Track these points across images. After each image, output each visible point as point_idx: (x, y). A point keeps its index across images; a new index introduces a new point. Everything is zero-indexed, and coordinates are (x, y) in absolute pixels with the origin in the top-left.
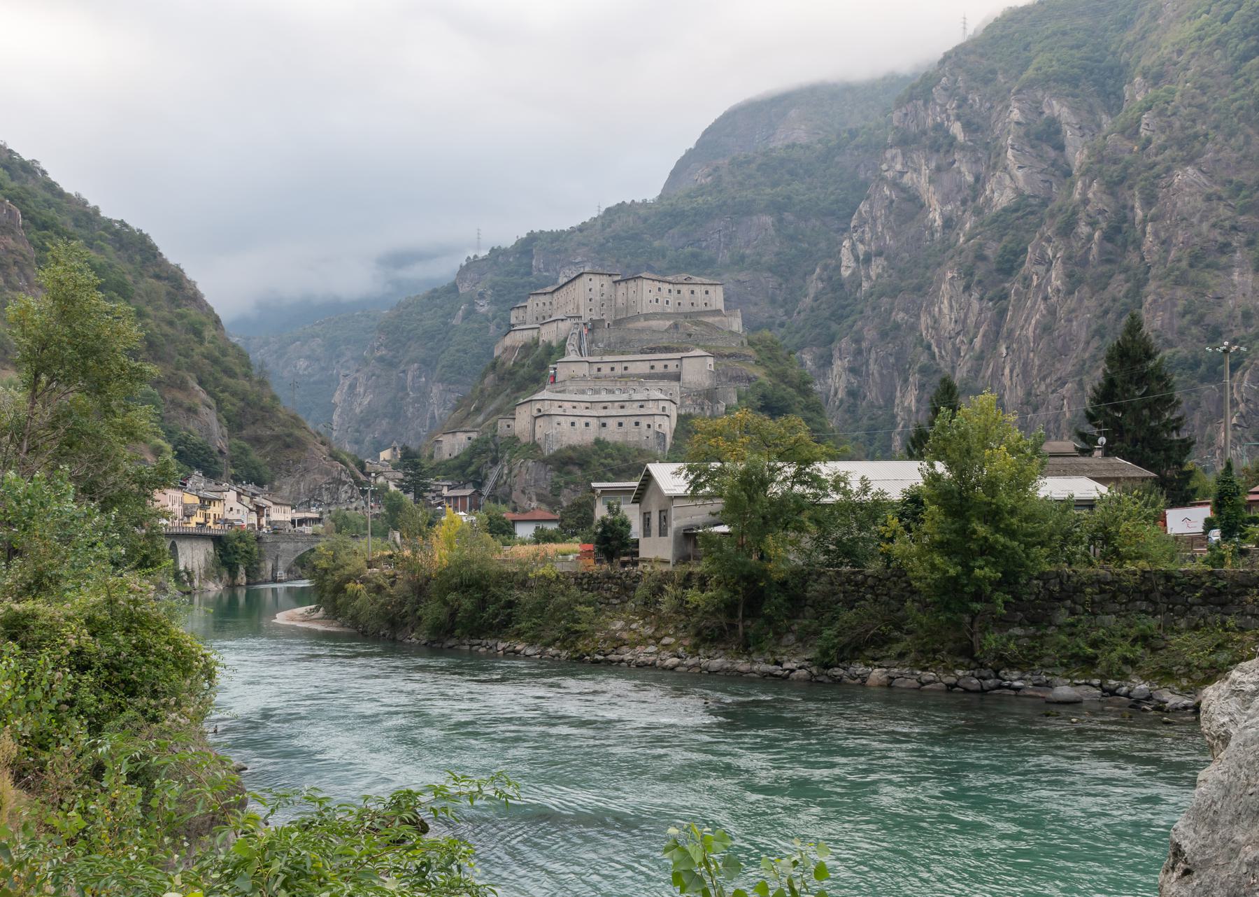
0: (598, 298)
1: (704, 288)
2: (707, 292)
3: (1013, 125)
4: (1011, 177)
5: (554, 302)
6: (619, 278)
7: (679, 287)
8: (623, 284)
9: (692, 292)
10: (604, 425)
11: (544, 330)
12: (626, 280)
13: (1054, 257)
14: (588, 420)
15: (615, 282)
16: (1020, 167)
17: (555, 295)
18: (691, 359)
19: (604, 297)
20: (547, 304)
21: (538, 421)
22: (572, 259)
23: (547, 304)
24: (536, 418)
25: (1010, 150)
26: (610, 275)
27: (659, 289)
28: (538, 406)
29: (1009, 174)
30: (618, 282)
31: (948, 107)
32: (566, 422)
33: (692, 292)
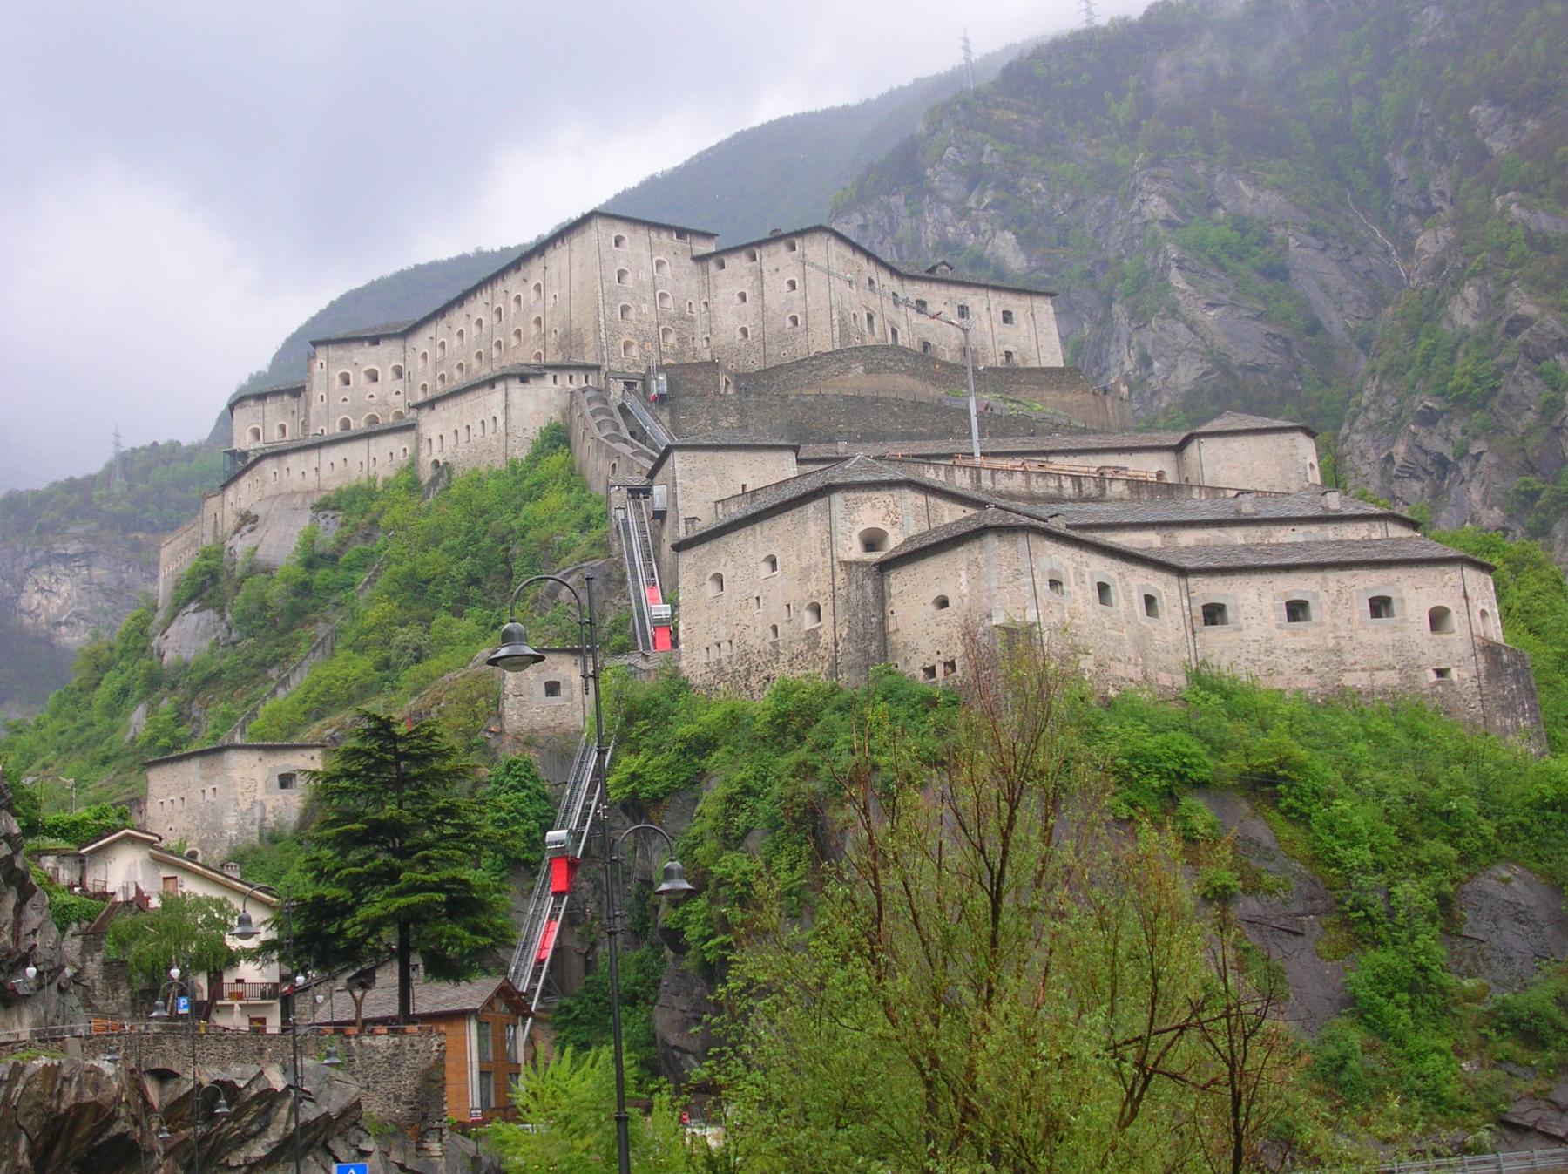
0: (645, 308)
1: (999, 301)
2: (1007, 317)
3: (1157, 226)
4: (1191, 327)
5: (416, 365)
6: (710, 247)
8: (738, 263)
10: (1214, 614)
11: (433, 425)
12: (750, 248)
13: (1463, 454)
14: (1158, 582)
15: (700, 259)
16: (1212, 306)
17: (422, 341)
18: (1237, 443)
19: (669, 303)
20: (386, 374)
21: (897, 582)
22: (59, 548)
23: (386, 374)
24: (886, 566)
25: (1177, 279)
26: (682, 233)
28: (871, 512)
29: (1185, 320)
30: (719, 257)
31: (972, 203)
32: (1079, 574)
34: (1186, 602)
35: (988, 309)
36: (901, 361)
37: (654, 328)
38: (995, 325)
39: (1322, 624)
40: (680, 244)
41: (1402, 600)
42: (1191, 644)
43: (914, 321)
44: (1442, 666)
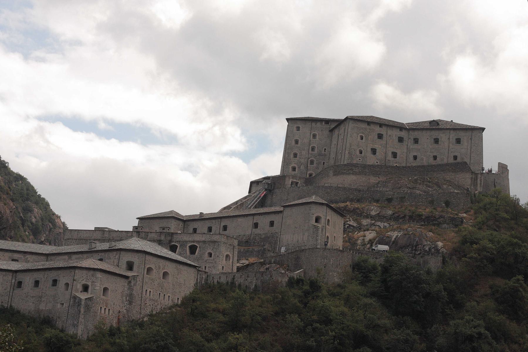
0: (304, 153)
2: (458, 141)
7: (416, 134)
9: (436, 141)
18: (294, 209)
27: (380, 136)
33: (436, 141)
34: (13, 281)
35: (449, 139)
36: (352, 169)
37: (306, 160)
38: (451, 145)
39: (40, 288)
40: (327, 126)
41: (59, 280)
42: (11, 294)
43: (411, 147)
44: (62, 303)
